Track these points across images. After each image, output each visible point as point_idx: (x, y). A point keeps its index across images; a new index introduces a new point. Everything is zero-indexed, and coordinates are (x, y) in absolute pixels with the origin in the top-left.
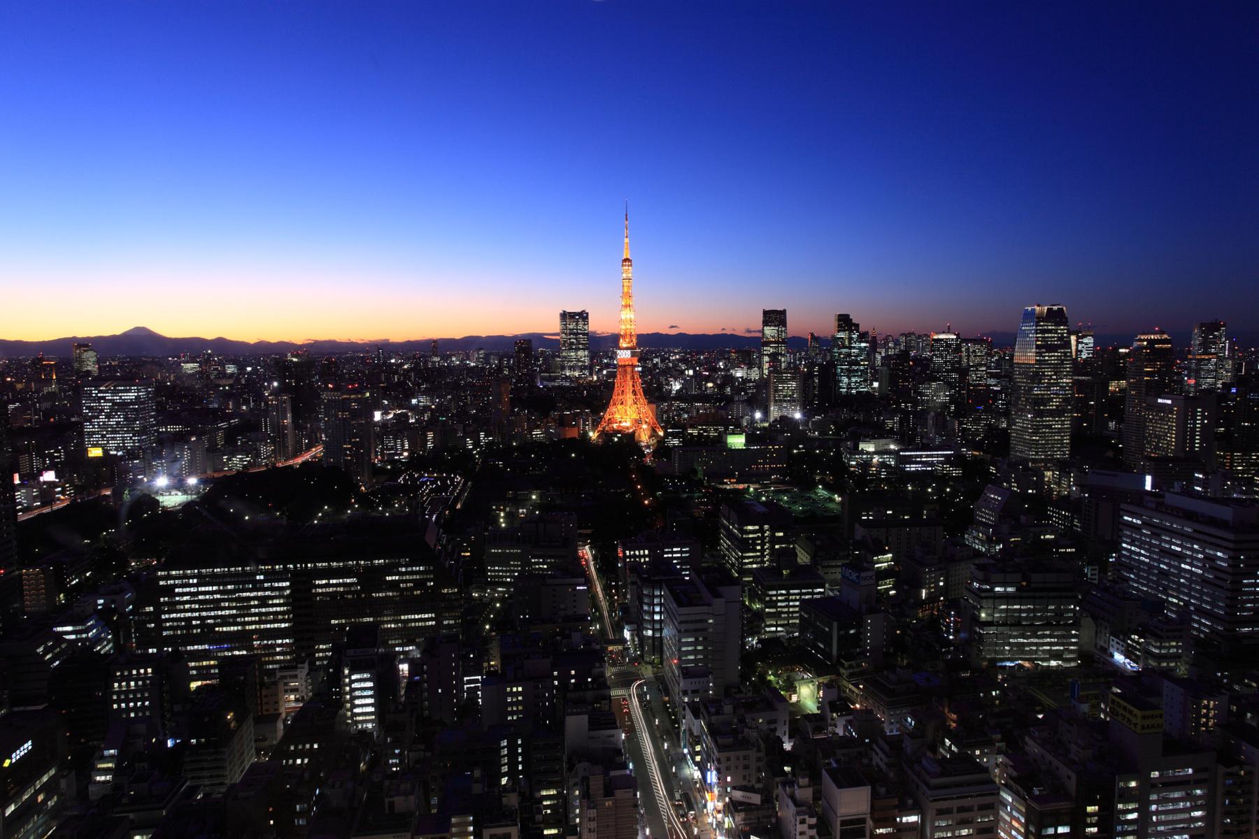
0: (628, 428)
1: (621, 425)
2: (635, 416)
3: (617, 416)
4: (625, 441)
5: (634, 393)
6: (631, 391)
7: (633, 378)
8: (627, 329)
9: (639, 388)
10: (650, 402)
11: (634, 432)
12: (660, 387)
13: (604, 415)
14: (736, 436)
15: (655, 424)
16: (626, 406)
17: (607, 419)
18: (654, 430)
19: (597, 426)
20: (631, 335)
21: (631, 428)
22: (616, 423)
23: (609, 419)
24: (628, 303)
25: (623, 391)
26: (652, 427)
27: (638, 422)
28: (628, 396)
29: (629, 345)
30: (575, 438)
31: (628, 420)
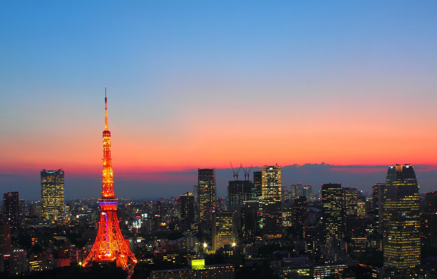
2: (114, 249)
6: (112, 230)
8: (108, 183)
10: (125, 238)
11: (115, 260)
14: (198, 260)
22: (100, 254)
23: (95, 252)
26: (128, 257)
27: (117, 254)
28: (110, 234)
31: (111, 252)
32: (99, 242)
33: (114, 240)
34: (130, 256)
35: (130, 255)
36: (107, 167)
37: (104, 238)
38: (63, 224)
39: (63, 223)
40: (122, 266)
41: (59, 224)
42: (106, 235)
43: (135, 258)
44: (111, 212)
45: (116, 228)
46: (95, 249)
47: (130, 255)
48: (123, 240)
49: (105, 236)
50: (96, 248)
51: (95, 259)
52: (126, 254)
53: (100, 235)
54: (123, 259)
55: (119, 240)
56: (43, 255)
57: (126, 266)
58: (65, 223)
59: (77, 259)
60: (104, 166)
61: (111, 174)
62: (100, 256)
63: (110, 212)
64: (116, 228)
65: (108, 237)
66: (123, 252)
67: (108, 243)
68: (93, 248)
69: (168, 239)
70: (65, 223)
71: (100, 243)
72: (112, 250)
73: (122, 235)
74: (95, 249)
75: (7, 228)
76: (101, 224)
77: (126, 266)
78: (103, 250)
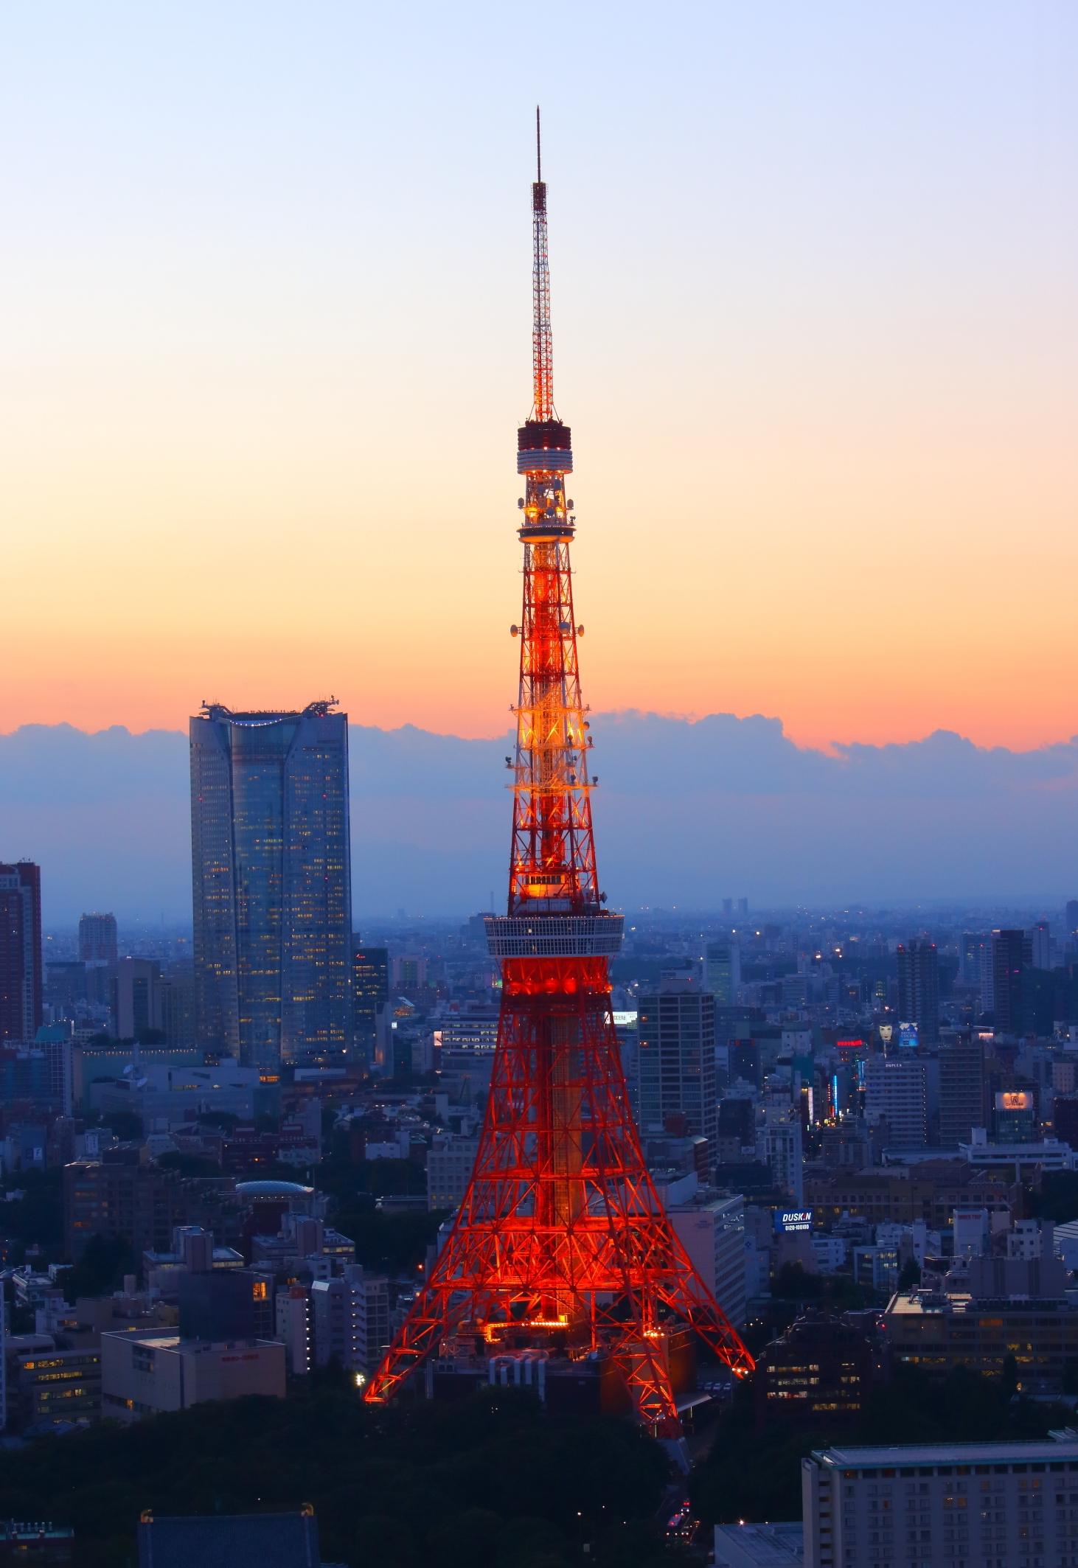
3: (505, 1279)
52: (686, 1321)
54: (649, 1358)
60: (522, 675)
67: (547, 1236)
72: (573, 1289)
78: (515, 1289)
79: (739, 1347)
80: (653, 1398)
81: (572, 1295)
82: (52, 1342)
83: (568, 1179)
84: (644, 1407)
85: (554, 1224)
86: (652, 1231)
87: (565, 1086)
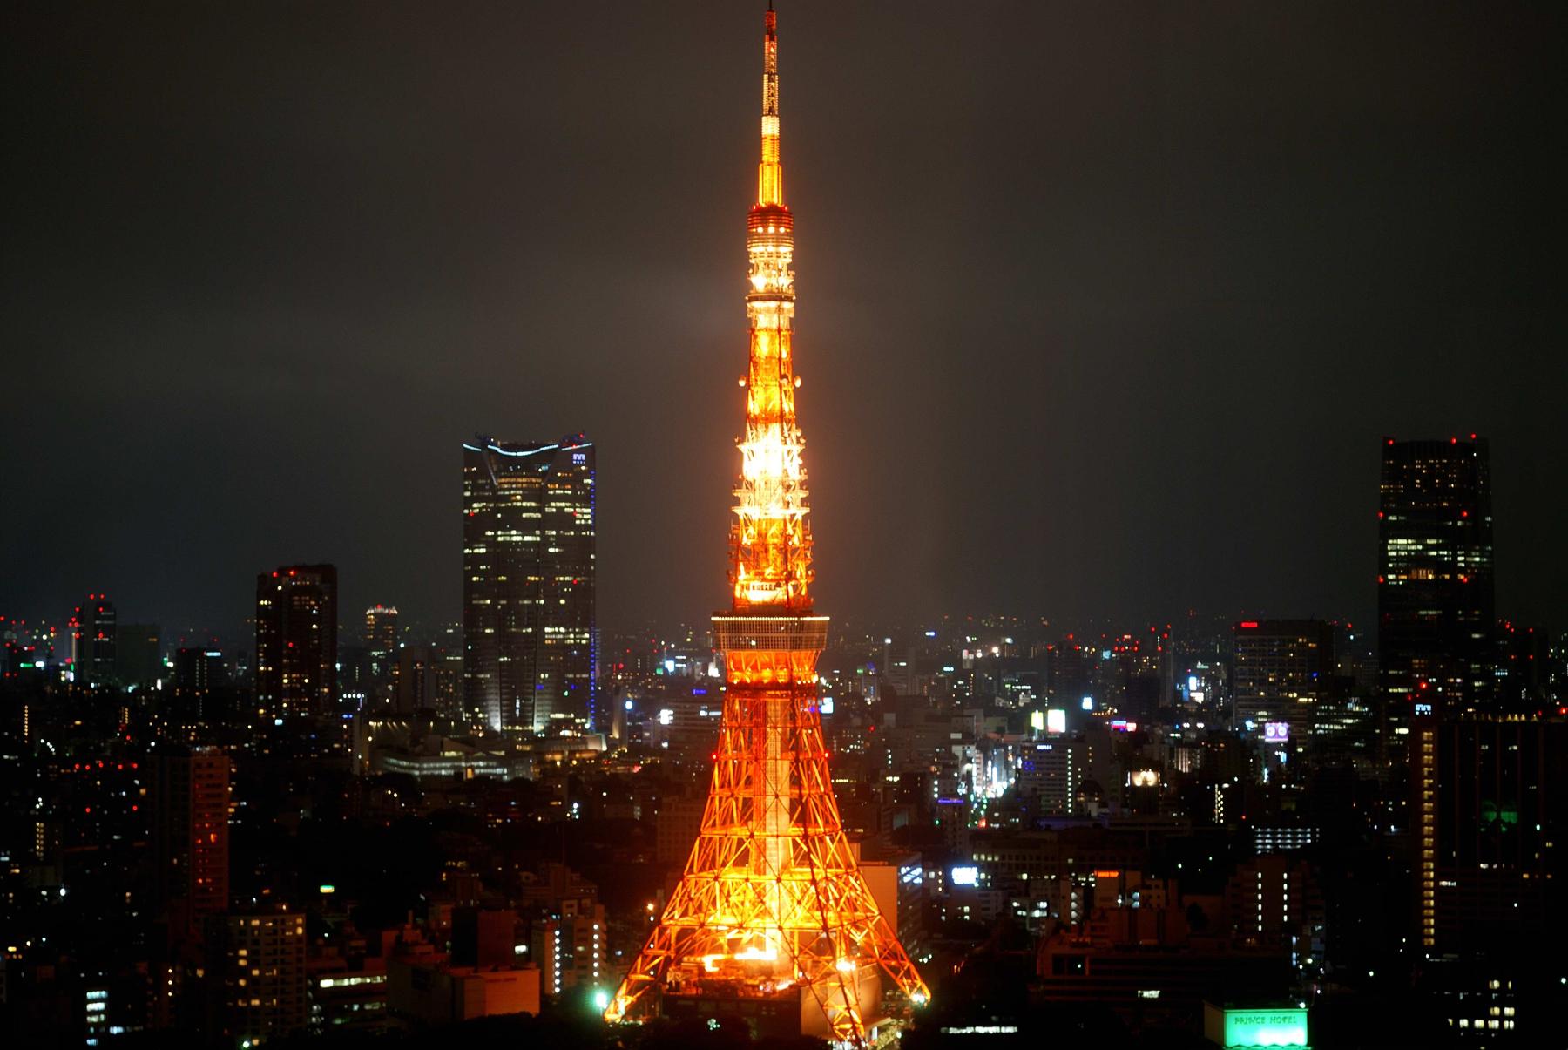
0: (768, 974)
1: (738, 957)
2: (803, 919)
3: (720, 918)
4: (754, 1034)
5: (801, 813)
6: (785, 802)
7: (792, 745)
8: (771, 522)
9: (818, 780)
11: (796, 991)
12: (915, 785)
13: (658, 913)
14: (1268, 1015)
15: (894, 956)
16: (760, 871)
17: (673, 932)
18: (886, 984)
19: (628, 965)
20: (786, 551)
21: (788, 972)
22: (717, 949)
23: (684, 933)
24: (775, 405)
25: (747, 803)
28: (771, 827)
29: (779, 594)
30: (525, 1015)
32: (709, 875)
33: (800, 865)
34: (893, 969)
35: (893, 963)
36: (767, 427)
37: (736, 853)
38: (578, 760)
39: (581, 752)
40: (832, 1025)
41: (558, 757)
42: (752, 836)
43: (924, 980)
44: (782, 696)
45: (813, 792)
46: (685, 914)
47: (893, 963)
48: (849, 866)
49: (747, 839)
50: (691, 910)
51: (680, 977)
52: (872, 957)
53: (716, 834)
54: (842, 986)
55: (829, 866)
56: (399, 939)
57: (855, 1029)
58: (593, 755)
59: (595, 970)
61: (787, 465)
62: (709, 962)
63: (776, 696)
64: (813, 792)
65: (762, 850)
66: (851, 943)
67: (760, 884)
68: (673, 910)
69: (1139, 873)
70: (590, 751)
71: (716, 879)
72: (780, 928)
73: (845, 839)
74: (685, 914)
75: (210, 776)
76: (726, 763)
77: (855, 1029)
78: (731, 927)
79: (915, 979)
80: (843, 1021)
81: (779, 932)
82: (539, 970)
83: (777, 836)
84: (837, 1027)
85: (765, 873)
86: (847, 883)
87: (776, 760)
